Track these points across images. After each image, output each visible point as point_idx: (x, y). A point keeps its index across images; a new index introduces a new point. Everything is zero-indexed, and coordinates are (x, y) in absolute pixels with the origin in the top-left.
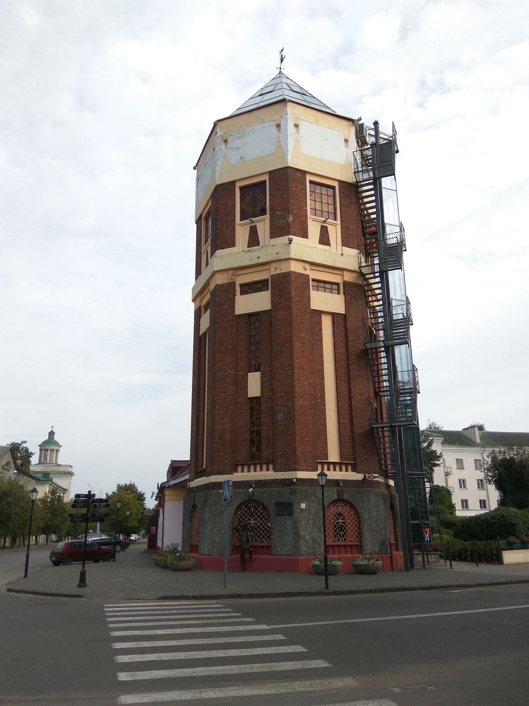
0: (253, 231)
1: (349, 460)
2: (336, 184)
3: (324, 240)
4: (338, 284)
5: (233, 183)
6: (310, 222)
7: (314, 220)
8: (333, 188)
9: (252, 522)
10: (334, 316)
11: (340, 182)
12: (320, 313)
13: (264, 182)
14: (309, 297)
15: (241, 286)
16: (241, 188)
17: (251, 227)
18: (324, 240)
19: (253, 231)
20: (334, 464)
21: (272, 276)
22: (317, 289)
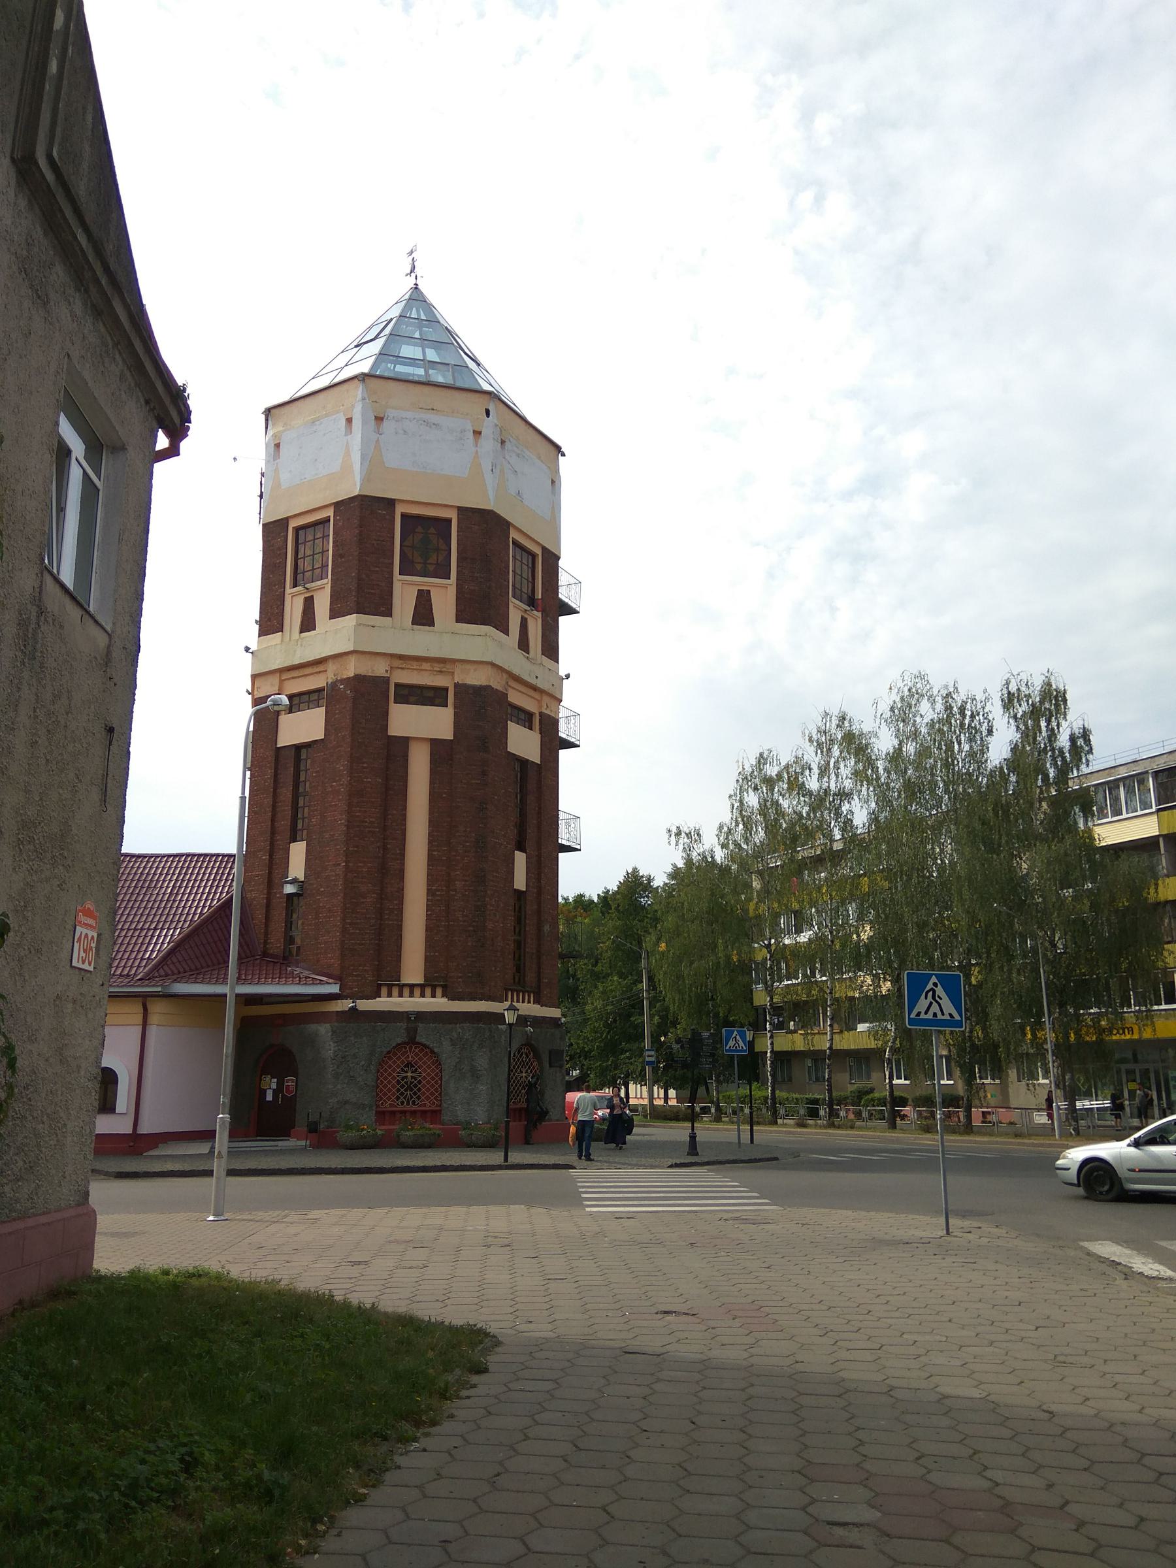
0: (309, 603)
1: (433, 982)
2: (453, 515)
3: (423, 615)
4: (446, 689)
7: (404, 583)
8: (449, 521)
10: (435, 743)
11: (461, 510)
12: (405, 741)
13: (327, 520)
14: (386, 714)
16: (297, 530)
17: (306, 599)
18: (423, 615)
19: (309, 603)
20: (412, 987)
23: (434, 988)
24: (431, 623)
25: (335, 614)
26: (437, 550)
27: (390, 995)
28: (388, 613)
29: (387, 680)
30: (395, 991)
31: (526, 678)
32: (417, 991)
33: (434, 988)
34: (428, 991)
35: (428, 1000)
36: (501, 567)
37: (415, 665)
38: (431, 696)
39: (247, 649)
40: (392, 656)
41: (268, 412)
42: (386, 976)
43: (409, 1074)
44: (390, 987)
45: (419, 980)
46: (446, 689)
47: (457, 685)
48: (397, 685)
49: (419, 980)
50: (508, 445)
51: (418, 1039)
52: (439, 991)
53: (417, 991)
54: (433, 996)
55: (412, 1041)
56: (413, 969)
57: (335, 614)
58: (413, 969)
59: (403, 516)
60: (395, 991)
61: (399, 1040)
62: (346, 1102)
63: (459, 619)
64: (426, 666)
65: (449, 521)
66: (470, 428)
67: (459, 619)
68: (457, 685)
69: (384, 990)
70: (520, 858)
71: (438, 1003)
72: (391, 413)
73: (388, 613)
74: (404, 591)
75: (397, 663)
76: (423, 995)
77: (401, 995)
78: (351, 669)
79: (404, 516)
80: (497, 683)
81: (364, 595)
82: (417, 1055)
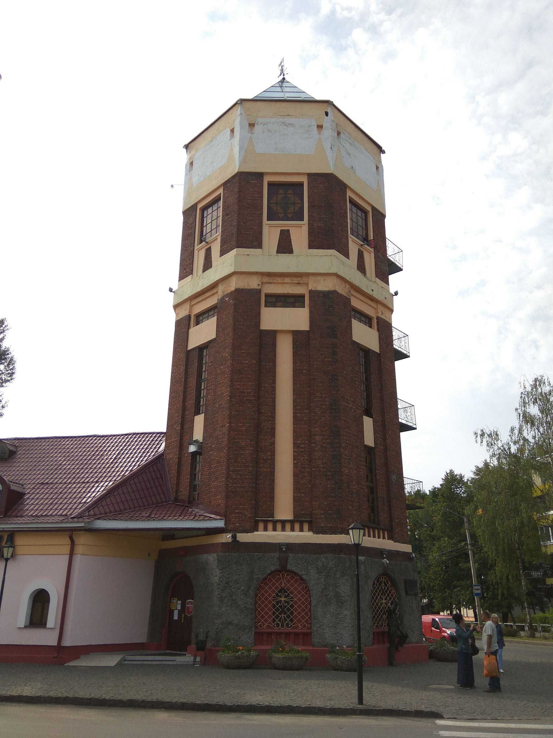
1: (300, 519)
3: (285, 246)
4: (303, 296)
8: (301, 185)
10: (296, 334)
11: (309, 175)
12: (273, 334)
14: (258, 315)
18: (285, 246)
20: (283, 522)
23: (301, 523)
24: (291, 251)
25: (223, 252)
26: (294, 203)
27: (266, 529)
28: (259, 246)
29: (259, 292)
30: (270, 526)
31: (364, 289)
32: (288, 526)
33: (301, 523)
34: (297, 526)
35: (297, 533)
37: (279, 280)
39: (171, 290)
40: (262, 274)
41: (187, 147)
42: (263, 515)
43: (283, 599)
44: (266, 522)
45: (290, 517)
46: (303, 296)
47: (311, 292)
48: (267, 296)
49: (290, 517)
50: (342, 135)
51: (289, 567)
52: (306, 526)
53: (288, 526)
54: (301, 530)
55: (283, 569)
56: (284, 508)
57: (223, 252)
58: (284, 508)
60: (270, 526)
61: (273, 569)
62: (230, 623)
63: (311, 247)
64: (287, 280)
65: (301, 185)
66: (314, 123)
67: (311, 247)
68: (311, 292)
69: (261, 526)
70: (368, 423)
71: (306, 536)
72: (260, 120)
73: (259, 246)
74: (271, 233)
75: (266, 279)
76: (293, 530)
77: (275, 529)
78: (233, 285)
79: (270, 184)
80: (342, 290)
81: (242, 234)
82: (288, 581)
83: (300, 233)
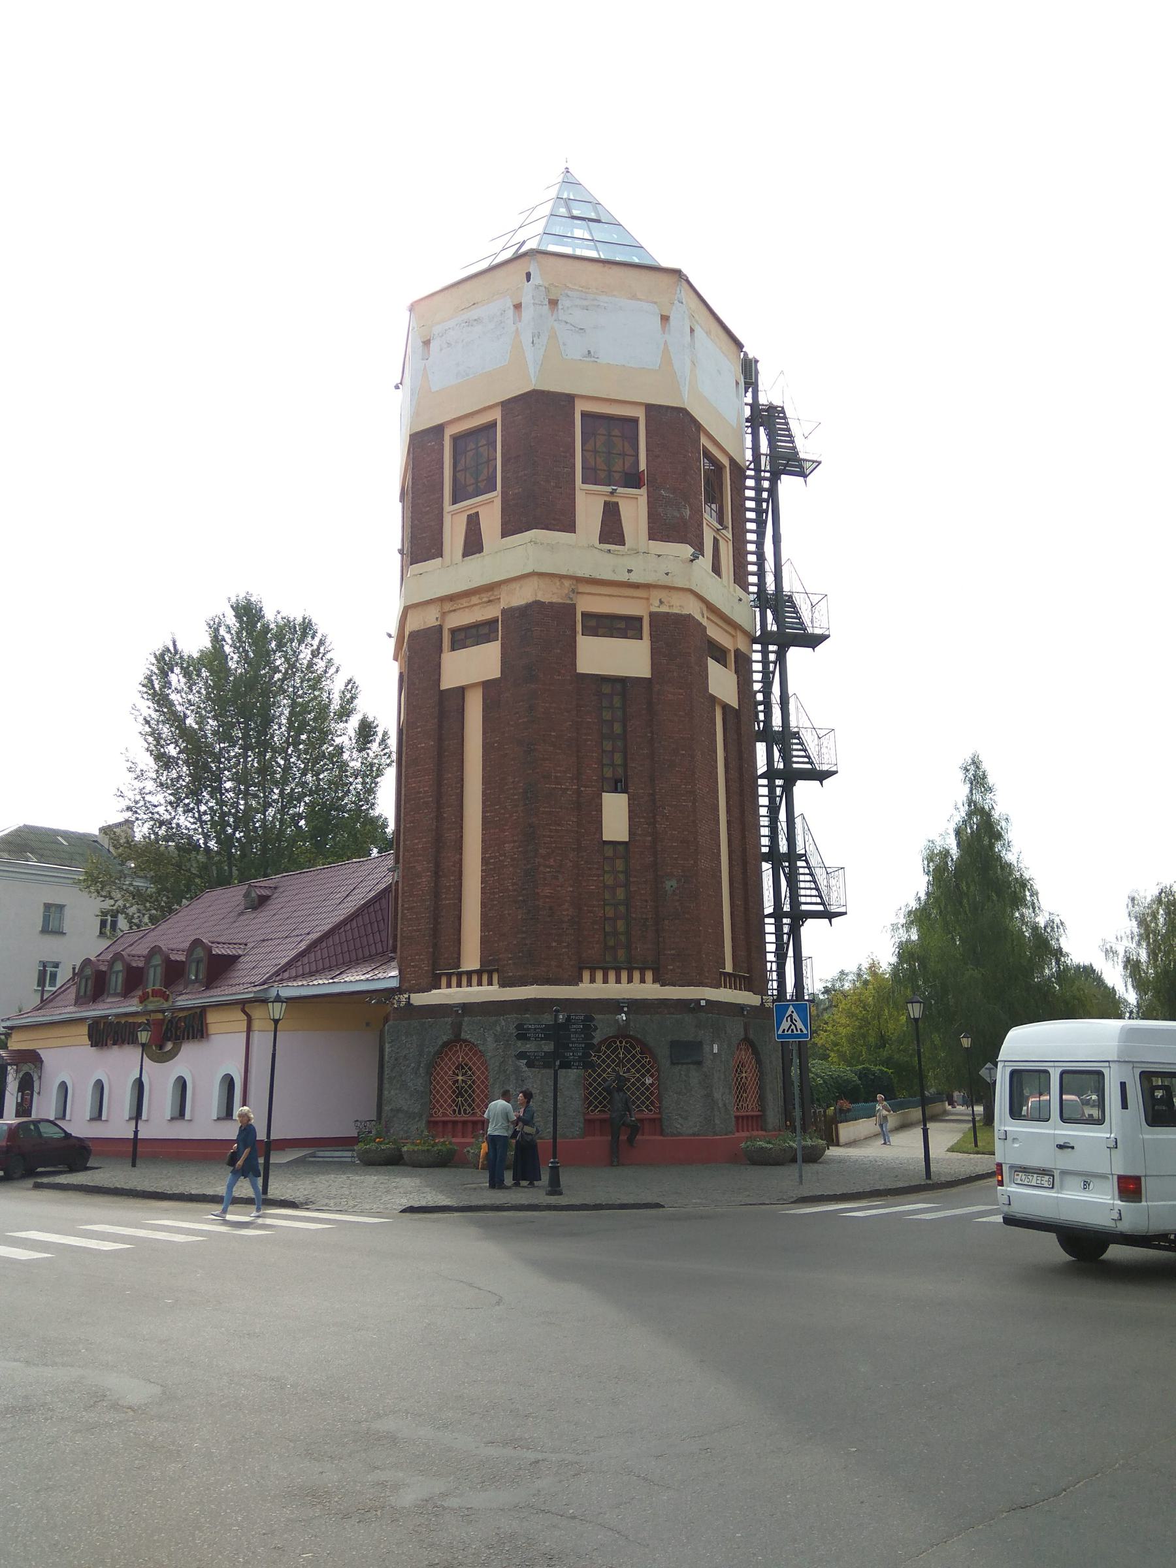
0: (473, 523)
2: (640, 413)
3: (612, 532)
4: (640, 619)
5: (439, 429)
6: (581, 499)
7: (588, 493)
8: (635, 421)
9: (460, 1078)
11: (650, 408)
15: (454, 632)
16: (456, 439)
18: (612, 532)
19: (473, 523)
21: (504, 611)
22: (590, 631)
25: (508, 530)
26: (623, 455)
28: (571, 528)
36: (702, 472)
38: (625, 627)
46: (640, 619)
47: (651, 615)
57: (508, 530)
59: (584, 415)
63: (652, 537)
65: (635, 421)
67: (652, 537)
68: (651, 615)
73: (571, 528)
74: (588, 505)
83: (635, 509)
